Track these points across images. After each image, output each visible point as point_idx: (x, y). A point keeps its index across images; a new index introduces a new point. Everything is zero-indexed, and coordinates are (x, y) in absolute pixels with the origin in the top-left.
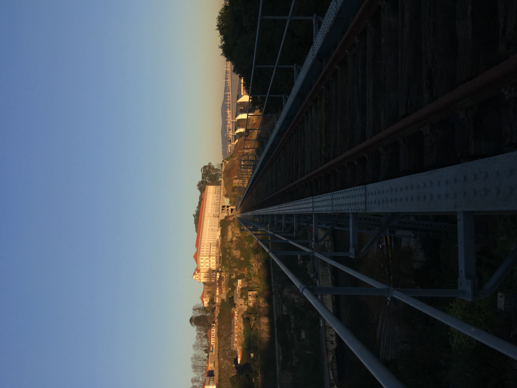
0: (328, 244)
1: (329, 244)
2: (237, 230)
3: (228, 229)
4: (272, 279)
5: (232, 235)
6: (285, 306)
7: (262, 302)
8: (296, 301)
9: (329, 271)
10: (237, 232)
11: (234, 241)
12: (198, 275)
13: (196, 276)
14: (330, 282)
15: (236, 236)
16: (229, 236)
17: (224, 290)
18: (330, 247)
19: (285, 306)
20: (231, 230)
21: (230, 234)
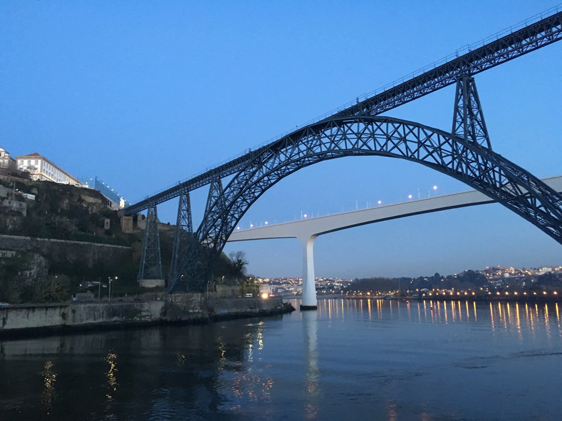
0: (147, 315)
1: (147, 317)
2: (97, 210)
3: (98, 198)
4: (55, 240)
5: (90, 202)
6: (13, 254)
7: (15, 221)
8: (28, 273)
9: (100, 320)
10: (94, 209)
11: (82, 204)
12: (5, 156)
13: (4, 152)
14: (84, 322)
15: (88, 207)
16: (88, 197)
17: (4, 178)
18: (143, 319)
19: (13, 254)
20: (96, 202)
21: (91, 200)
